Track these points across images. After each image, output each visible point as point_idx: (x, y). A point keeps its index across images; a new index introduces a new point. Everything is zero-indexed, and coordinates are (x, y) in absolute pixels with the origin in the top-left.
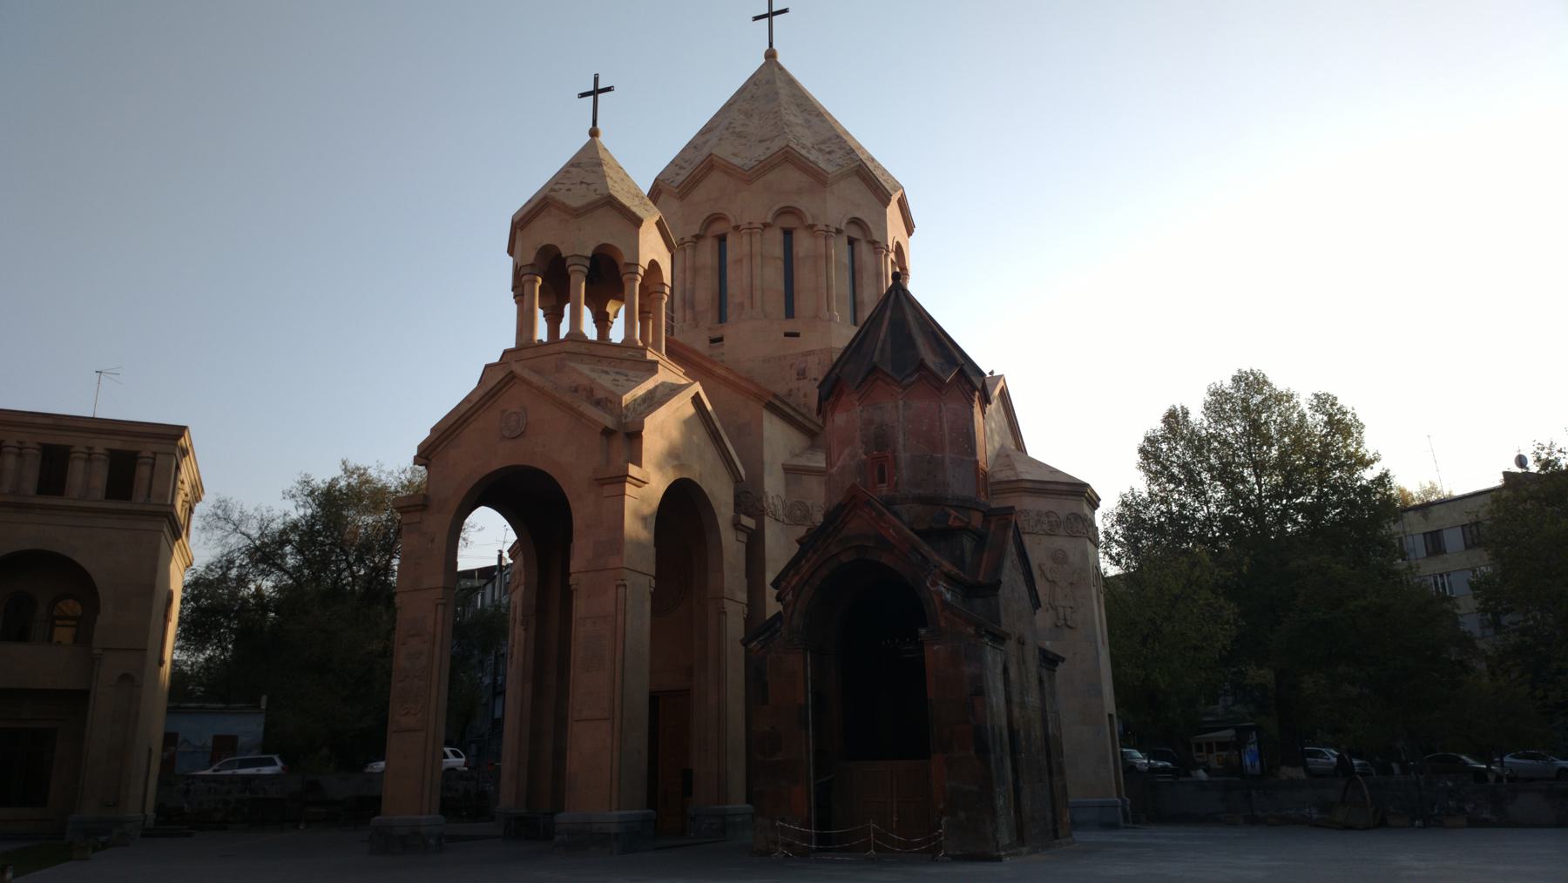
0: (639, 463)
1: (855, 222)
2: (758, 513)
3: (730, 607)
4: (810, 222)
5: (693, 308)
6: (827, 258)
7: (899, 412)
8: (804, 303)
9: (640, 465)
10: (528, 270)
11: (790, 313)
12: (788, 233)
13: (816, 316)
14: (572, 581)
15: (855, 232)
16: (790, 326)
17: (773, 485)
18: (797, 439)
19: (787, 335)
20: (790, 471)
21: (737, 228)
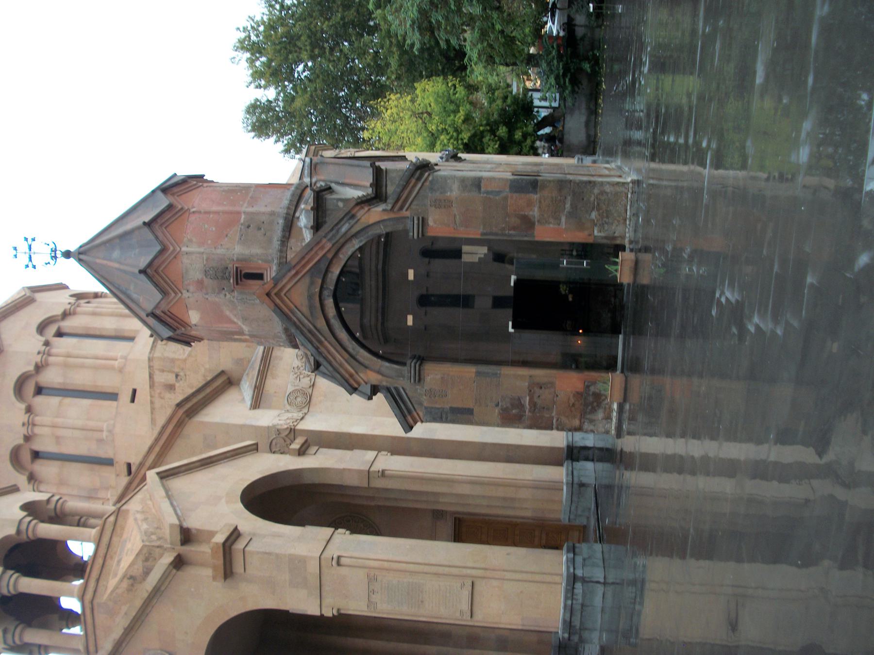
0: (212, 534)
1: (41, 328)
2: (293, 432)
3: (379, 466)
4: (31, 368)
5: (96, 490)
6: (69, 356)
7: (194, 253)
8: (106, 382)
9: (216, 532)
10: (9, 636)
11: (112, 396)
12: (39, 390)
13: (121, 370)
14: (328, 613)
15: (52, 329)
16: (126, 397)
17: (268, 418)
18: (231, 395)
19: (133, 400)
20: (257, 404)
21: (27, 438)
